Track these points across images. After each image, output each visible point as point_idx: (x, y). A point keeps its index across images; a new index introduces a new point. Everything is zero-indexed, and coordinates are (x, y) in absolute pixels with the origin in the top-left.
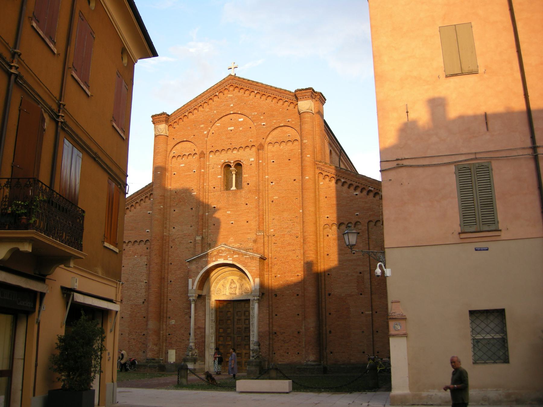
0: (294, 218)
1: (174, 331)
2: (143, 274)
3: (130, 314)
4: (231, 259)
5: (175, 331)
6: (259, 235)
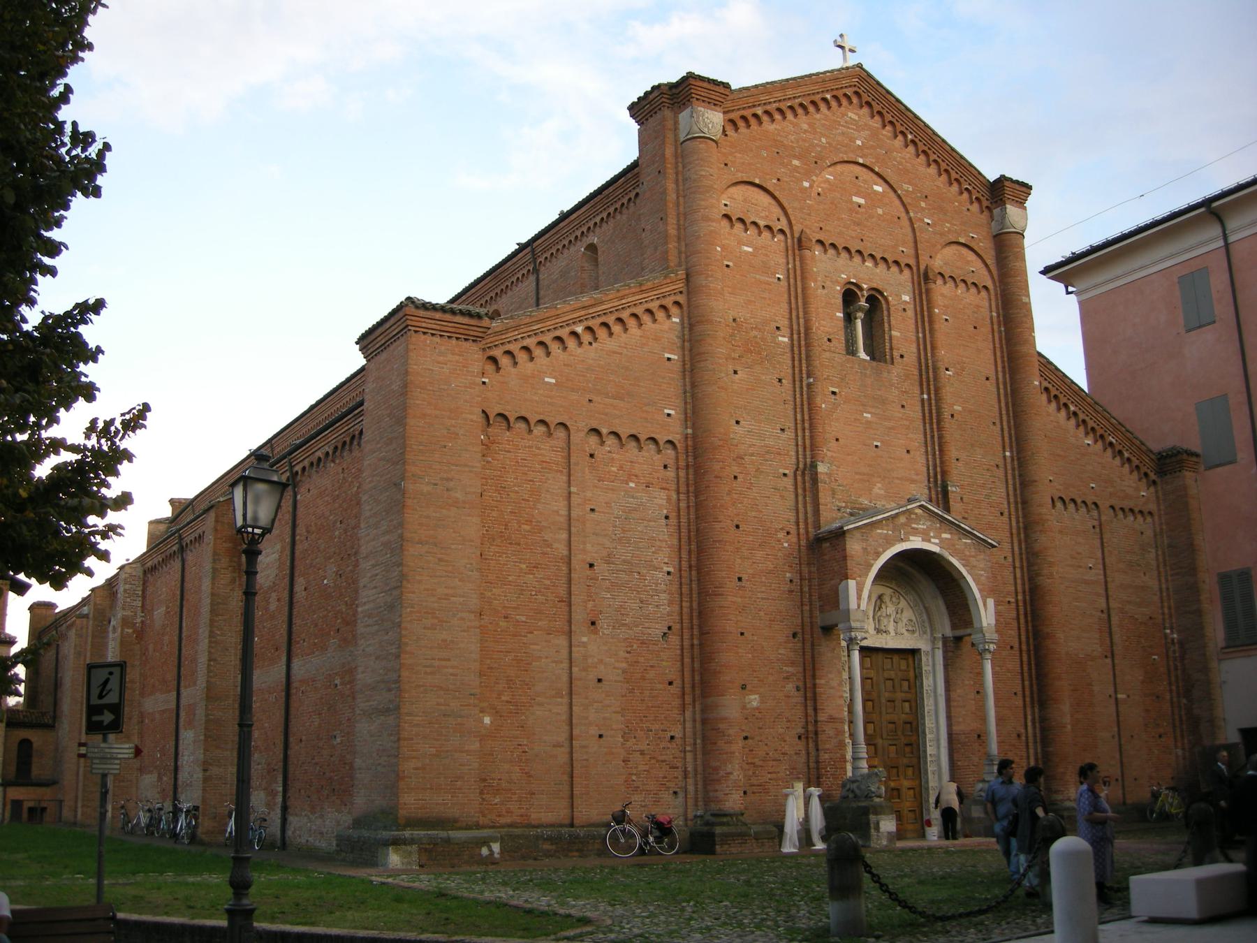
0: (992, 466)
1: (760, 728)
2: (658, 543)
3: (624, 672)
4: (937, 541)
5: (761, 728)
6: (953, 492)
